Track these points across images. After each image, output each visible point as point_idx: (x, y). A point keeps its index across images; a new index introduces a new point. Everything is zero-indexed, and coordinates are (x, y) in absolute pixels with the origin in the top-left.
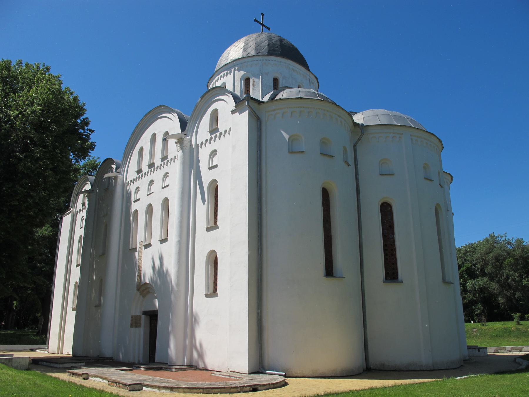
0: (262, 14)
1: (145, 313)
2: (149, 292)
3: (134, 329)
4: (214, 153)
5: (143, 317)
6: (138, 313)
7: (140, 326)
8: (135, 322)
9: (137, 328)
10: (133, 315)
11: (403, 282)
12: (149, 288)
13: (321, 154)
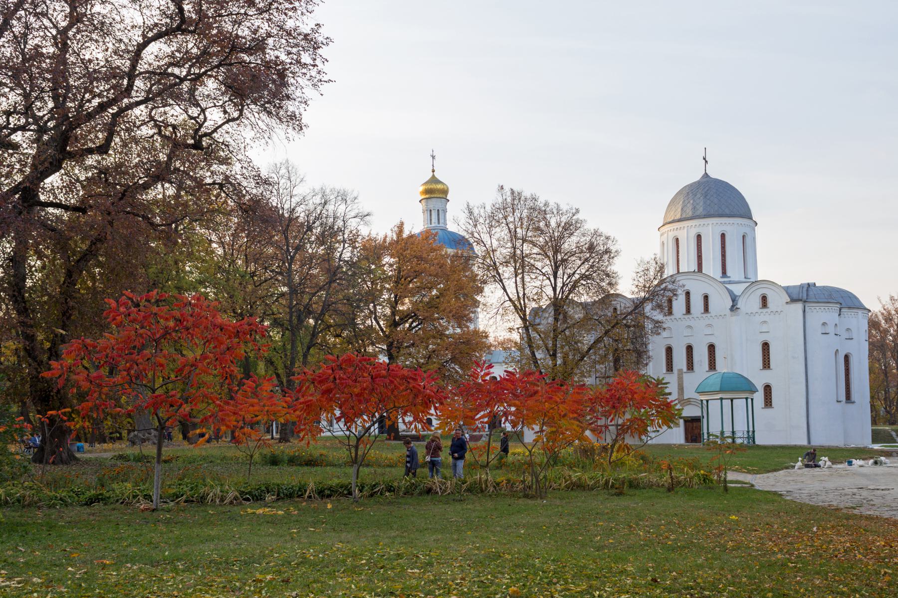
4: (765, 322)
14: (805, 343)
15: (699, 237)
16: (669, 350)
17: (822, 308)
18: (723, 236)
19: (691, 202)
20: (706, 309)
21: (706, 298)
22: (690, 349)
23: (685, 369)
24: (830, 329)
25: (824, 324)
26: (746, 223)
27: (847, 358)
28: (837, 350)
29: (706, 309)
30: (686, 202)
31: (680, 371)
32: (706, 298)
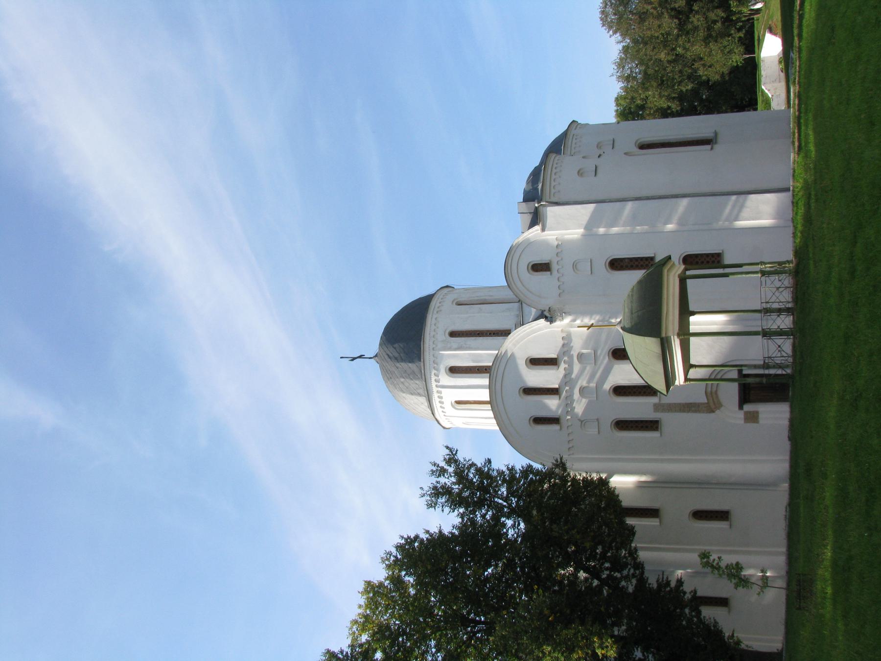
0: (341, 358)
1: (741, 407)
2: (716, 391)
3: (761, 421)
4: (575, 266)
5: (748, 407)
6: (741, 414)
7: (757, 412)
8: (752, 418)
9: (760, 416)
10: (743, 422)
11: (715, 131)
12: (711, 392)
13: (599, 156)
14: (611, 201)
15: (454, 370)
16: (622, 425)
17: (553, 177)
18: (453, 334)
19: (402, 380)
20: (551, 362)
21: (535, 362)
22: (620, 391)
23: (654, 400)
24: (590, 165)
25: (580, 173)
26: (441, 297)
27: (644, 146)
28: (625, 154)
29: (551, 362)
30: (401, 386)
31: (657, 407)
32: (535, 362)
